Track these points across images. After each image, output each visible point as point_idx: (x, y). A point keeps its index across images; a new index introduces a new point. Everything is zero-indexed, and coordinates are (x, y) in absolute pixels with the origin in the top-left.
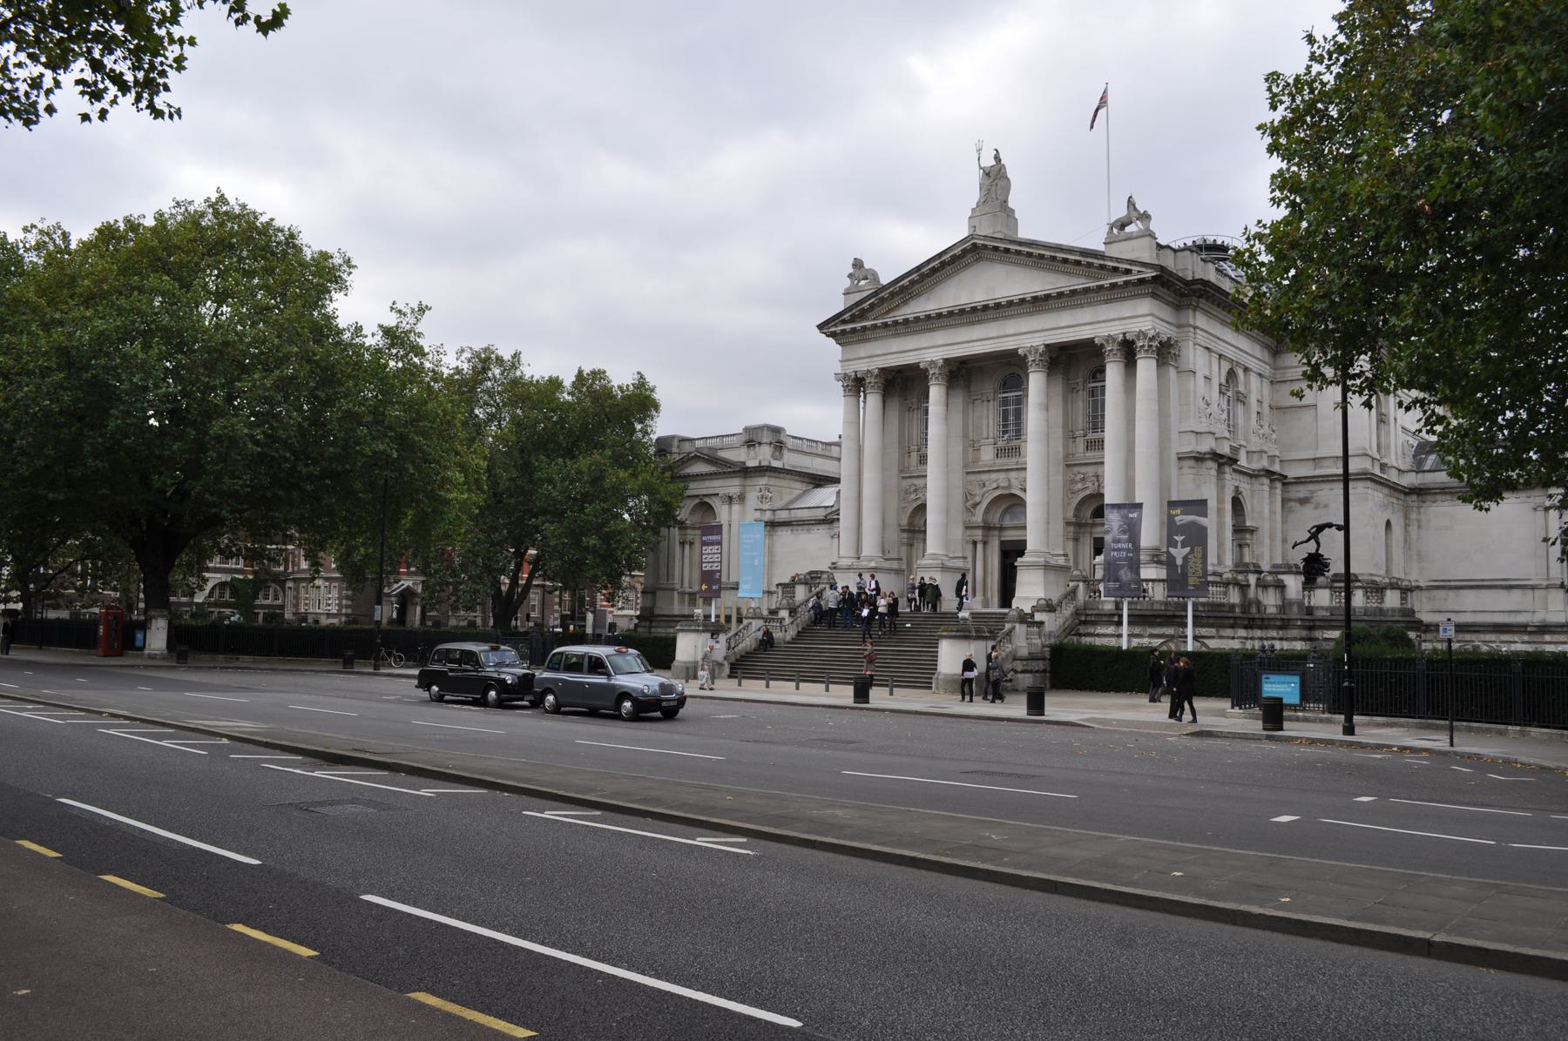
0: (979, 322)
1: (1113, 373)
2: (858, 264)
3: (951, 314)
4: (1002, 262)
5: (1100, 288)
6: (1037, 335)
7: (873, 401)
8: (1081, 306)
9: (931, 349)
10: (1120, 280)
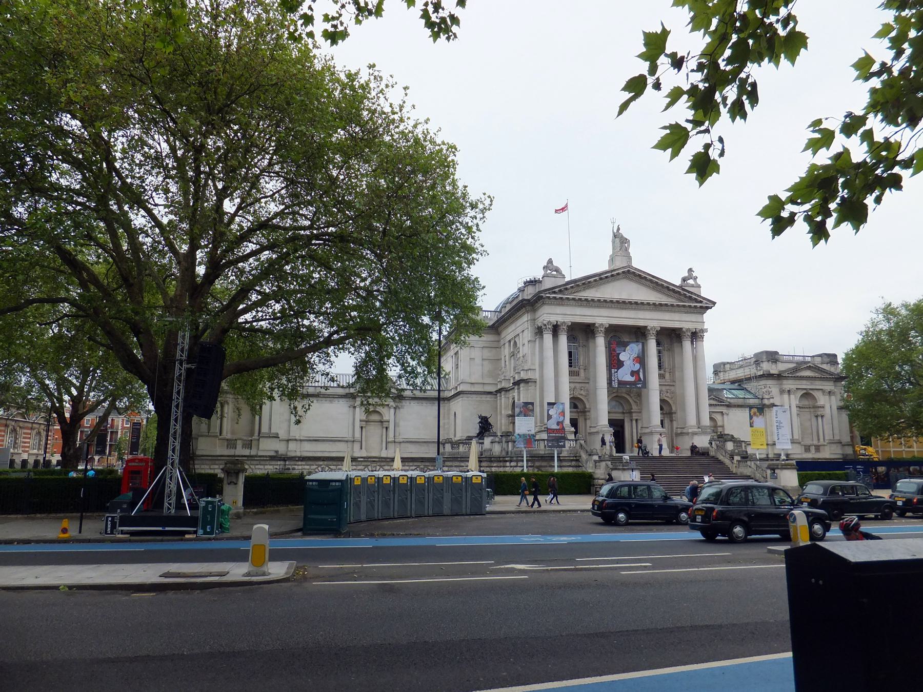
0: (625, 309)
2: (550, 261)
3: (618, 302)
5: (684, 306)
6: (654, 321)
7: (563, 339)
8: (675, 312)
9: (602, 318)
10: (699, 305)
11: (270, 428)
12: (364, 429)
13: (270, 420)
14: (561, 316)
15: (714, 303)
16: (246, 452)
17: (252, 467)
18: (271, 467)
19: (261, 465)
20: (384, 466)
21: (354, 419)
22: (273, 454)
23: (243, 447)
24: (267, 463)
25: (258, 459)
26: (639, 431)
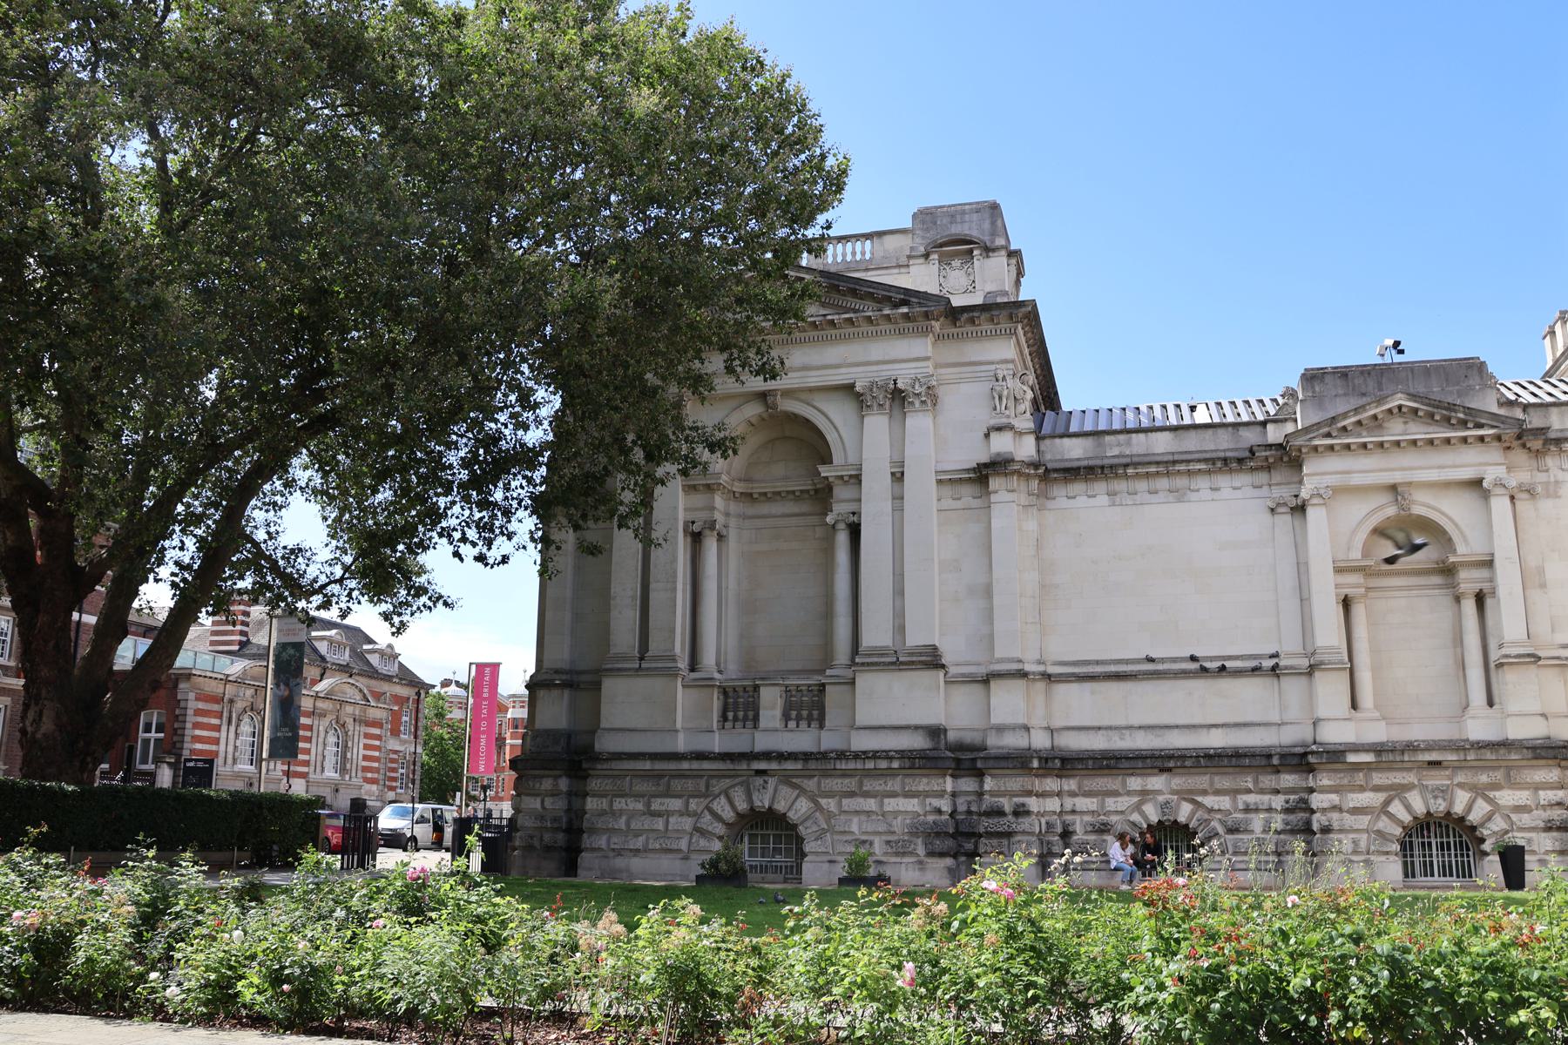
11: (900, 629)
12: (1359, 611)
13: (899, 592)
16: (801, 739)
17: (829, 804)
18: (912, 805)
19: (867, 795)
20: (1496, 787)
21: (1302, 568)
22: (918, 742)
23: (786, 717)
24: (894, 784)
25: (851, 765)
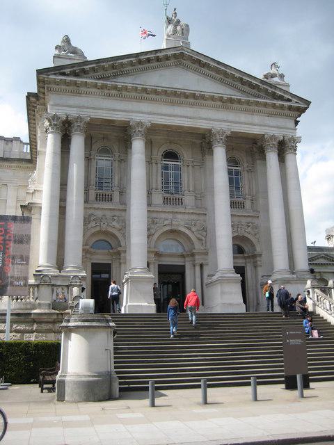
1: (272, 158)
2: (67, 40)
4: (195, 71)
10: (286, 104)
14: (75, 109)
15: (308, 103)
26: (205, 281)
